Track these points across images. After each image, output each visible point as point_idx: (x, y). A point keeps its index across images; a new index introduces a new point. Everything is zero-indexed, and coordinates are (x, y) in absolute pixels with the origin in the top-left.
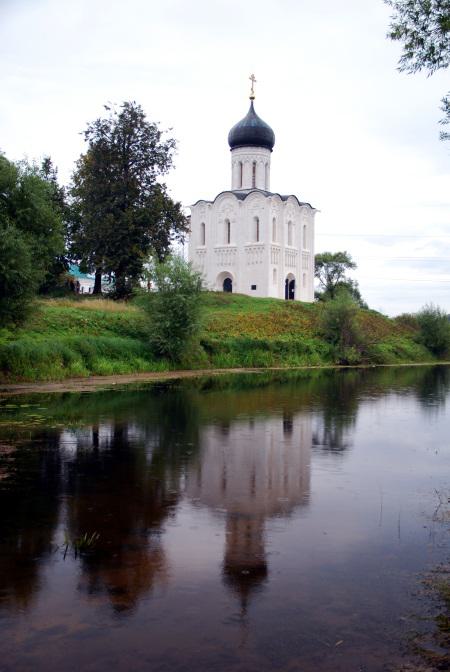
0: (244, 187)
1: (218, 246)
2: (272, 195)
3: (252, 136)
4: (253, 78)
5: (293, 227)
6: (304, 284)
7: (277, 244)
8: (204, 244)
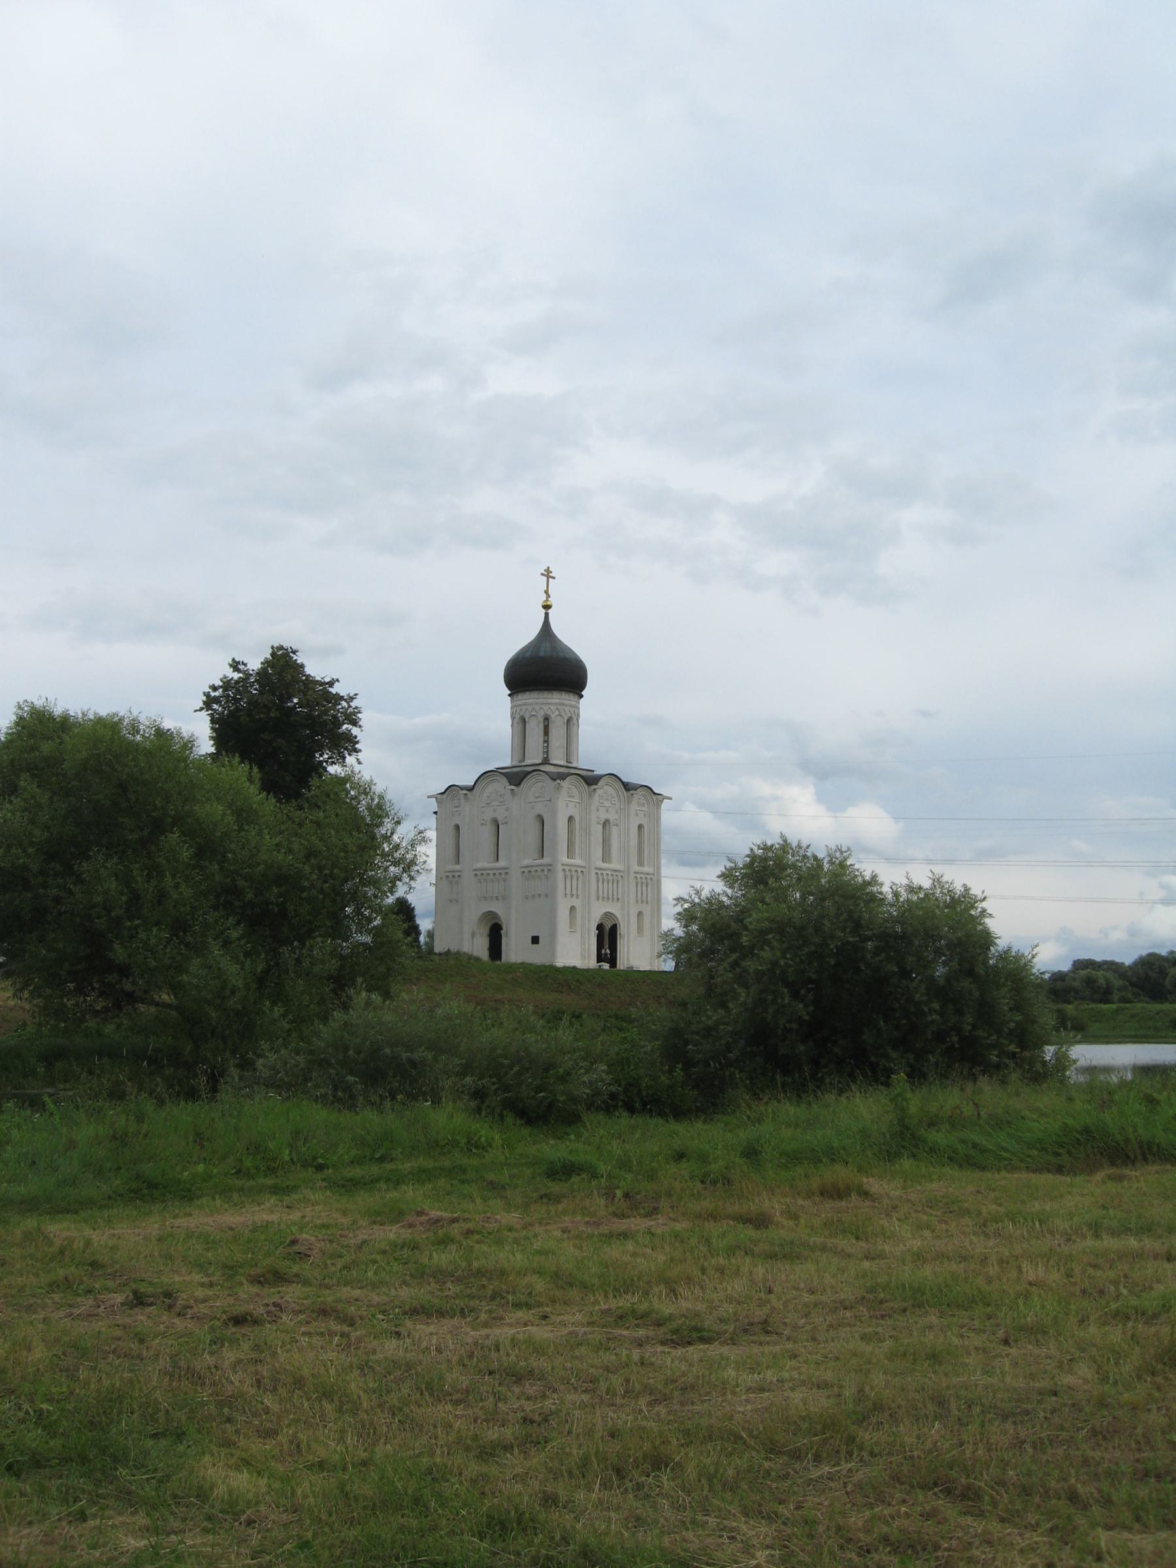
0: (528, 762)
1: (479, 865)
3: (546, 672)
4: (548, 574)
5: (614, 831)
6: (640, 930)
8: (458, 863)
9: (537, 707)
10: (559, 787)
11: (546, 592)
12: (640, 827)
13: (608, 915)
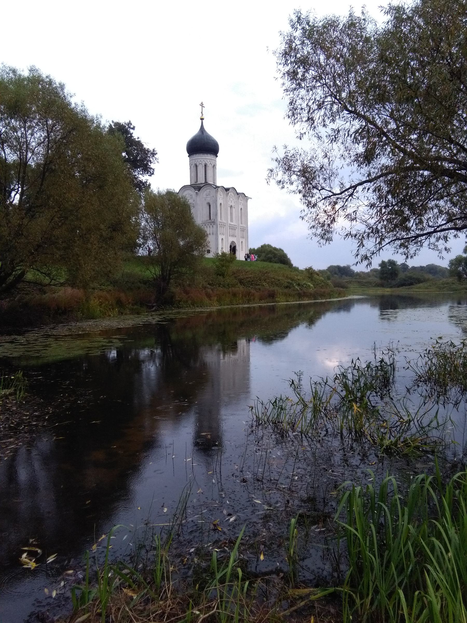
0: (199, 182)
2: (219, 187)
4: (202, 105)
5: (234, 210)
6: (242, 248)
7: (224, 221)
9: (202, 160)
10: (217, 191)
11: (202, 113)
12: (241, 209)
13: (233, 242)
